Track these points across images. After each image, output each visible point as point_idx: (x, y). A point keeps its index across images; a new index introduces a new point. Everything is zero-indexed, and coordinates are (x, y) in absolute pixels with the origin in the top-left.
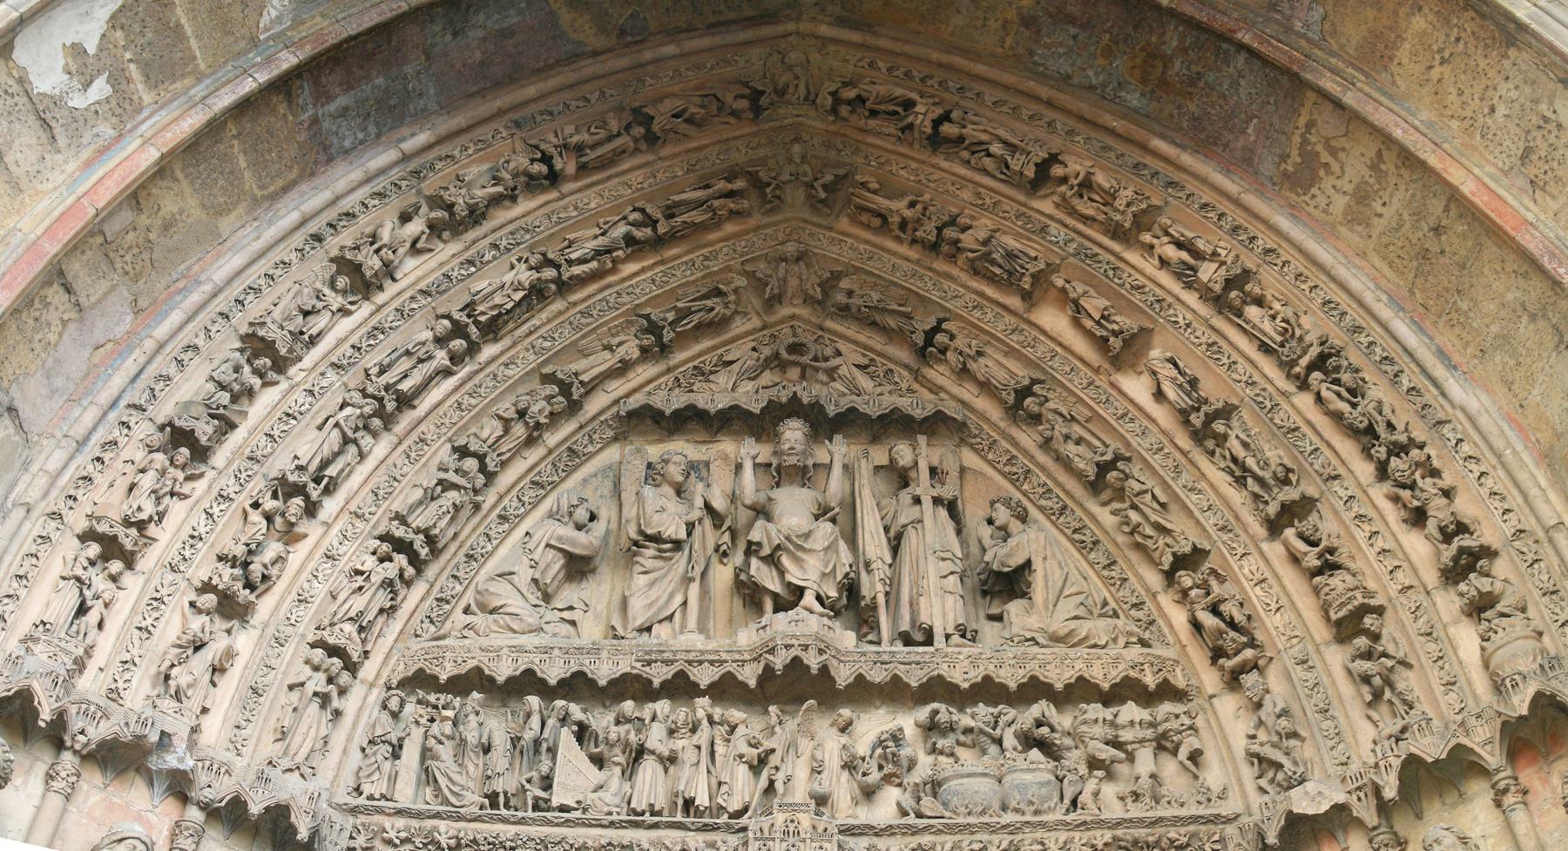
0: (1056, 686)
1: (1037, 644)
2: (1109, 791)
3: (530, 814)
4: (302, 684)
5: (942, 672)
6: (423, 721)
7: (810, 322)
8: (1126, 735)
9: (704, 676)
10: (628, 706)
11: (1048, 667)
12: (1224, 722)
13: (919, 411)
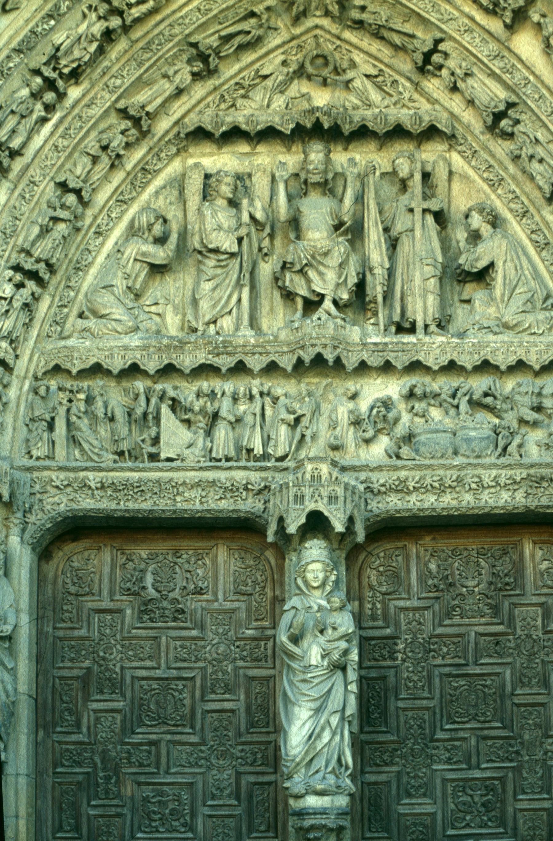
5: (420, 358)
6: (65, 402)
7: (329, 32)
10: (205, 385)
13: (416, 127)
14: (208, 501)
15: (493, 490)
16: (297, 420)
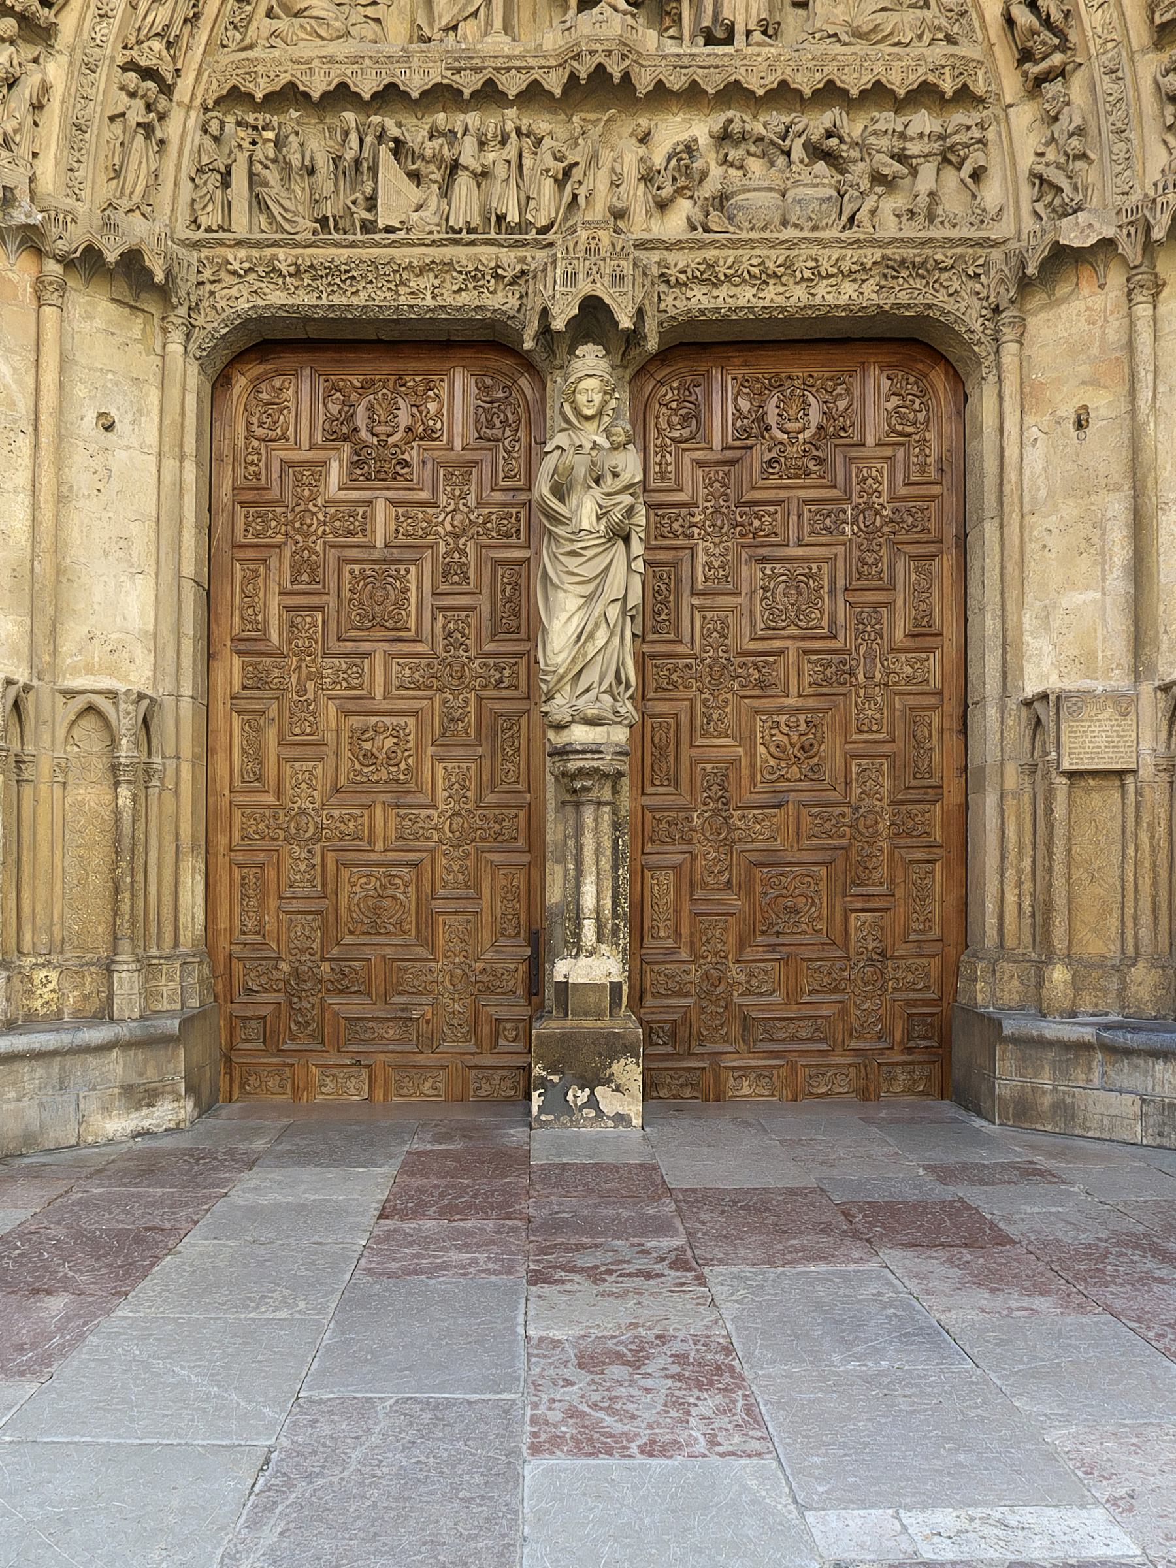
0: (852, 92)
1: (839, 41)
2: (891, 204)
3: (359, 237)
4: (123, 115)
8: (913, 148)
9: (512, 85)
11: (846, 71)
12: (1015, 135)
14: (442, 295)
15: (832, 281)
16: (567, 173)
